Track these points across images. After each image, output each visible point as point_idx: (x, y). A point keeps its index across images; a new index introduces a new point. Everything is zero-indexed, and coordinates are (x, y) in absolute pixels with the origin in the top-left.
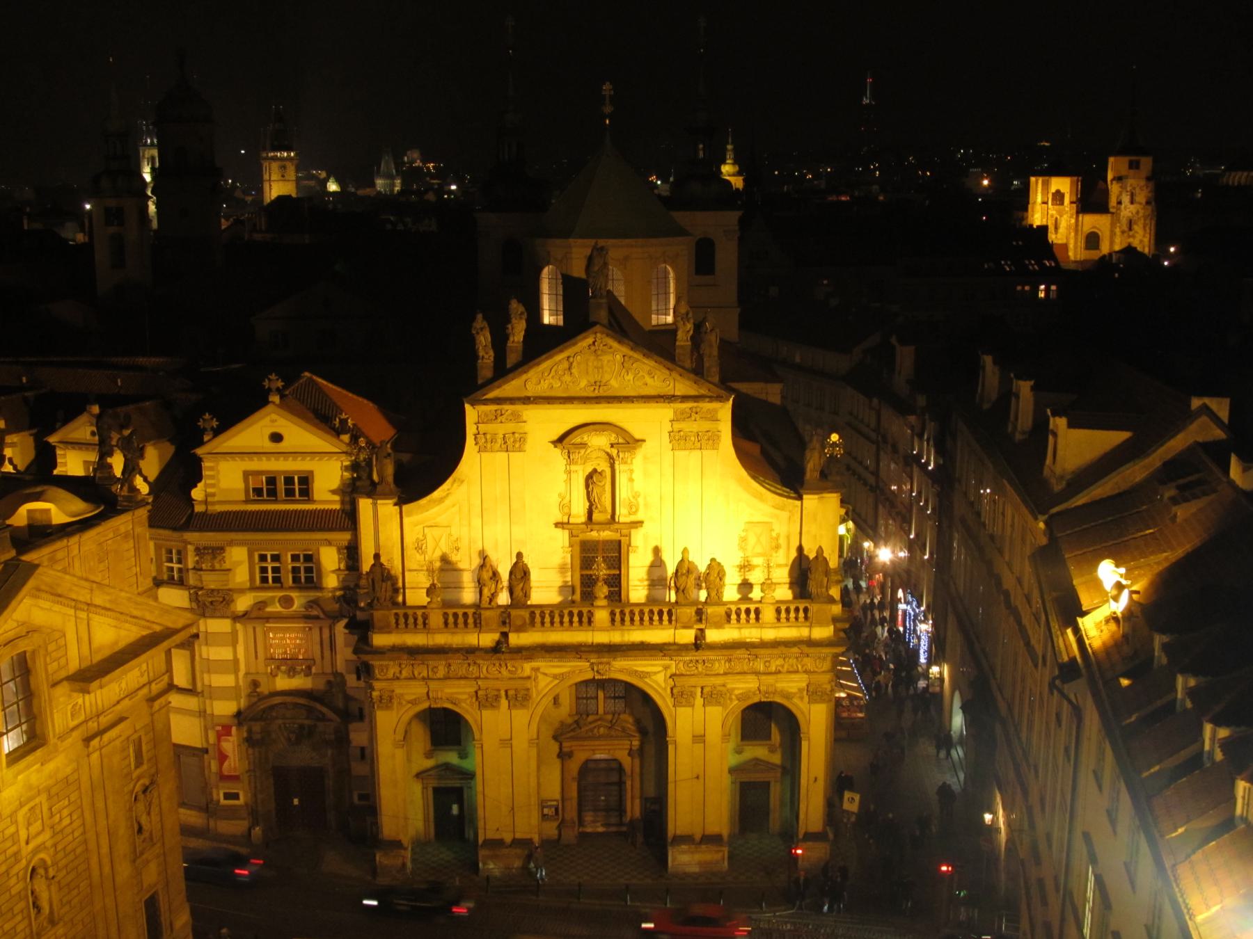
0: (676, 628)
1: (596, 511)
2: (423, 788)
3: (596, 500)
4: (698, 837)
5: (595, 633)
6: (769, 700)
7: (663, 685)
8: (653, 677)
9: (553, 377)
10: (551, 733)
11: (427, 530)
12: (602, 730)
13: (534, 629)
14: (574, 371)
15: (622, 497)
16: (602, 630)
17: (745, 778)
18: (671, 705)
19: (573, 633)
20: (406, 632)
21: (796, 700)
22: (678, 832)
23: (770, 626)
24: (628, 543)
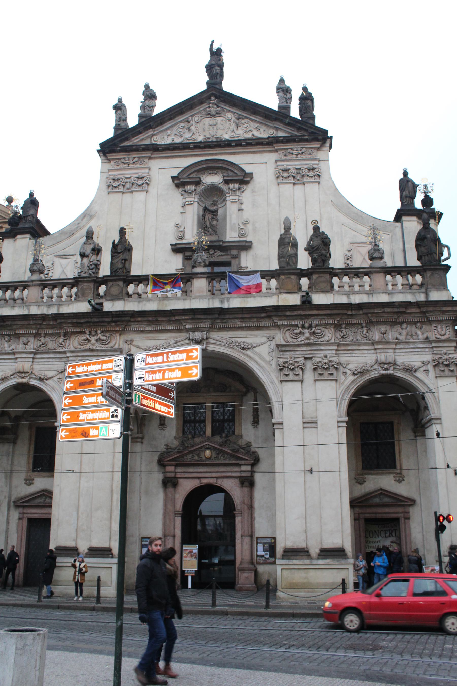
0: (280, 293)
1: (208, 233)
2: (20, 519)
3: (208, 225)
4: (314, 551)
5: (193, 301)
6: (388, 372)
7: (268, 358)
8: (256, 349)
9: (175, 135)
10: (156, 458)
11: (57, 260)
12: (208, 453)
13: (130, 299)
14: (193, 128)
15: (233, 222)
16: (201, 297)
17: (370, 513)
18: (276, 381)
19: (170, 301)
20: (5, 307)
21: (420, 374)
22: (290, 544)
23: (382, 292)
24: (237, 262)
